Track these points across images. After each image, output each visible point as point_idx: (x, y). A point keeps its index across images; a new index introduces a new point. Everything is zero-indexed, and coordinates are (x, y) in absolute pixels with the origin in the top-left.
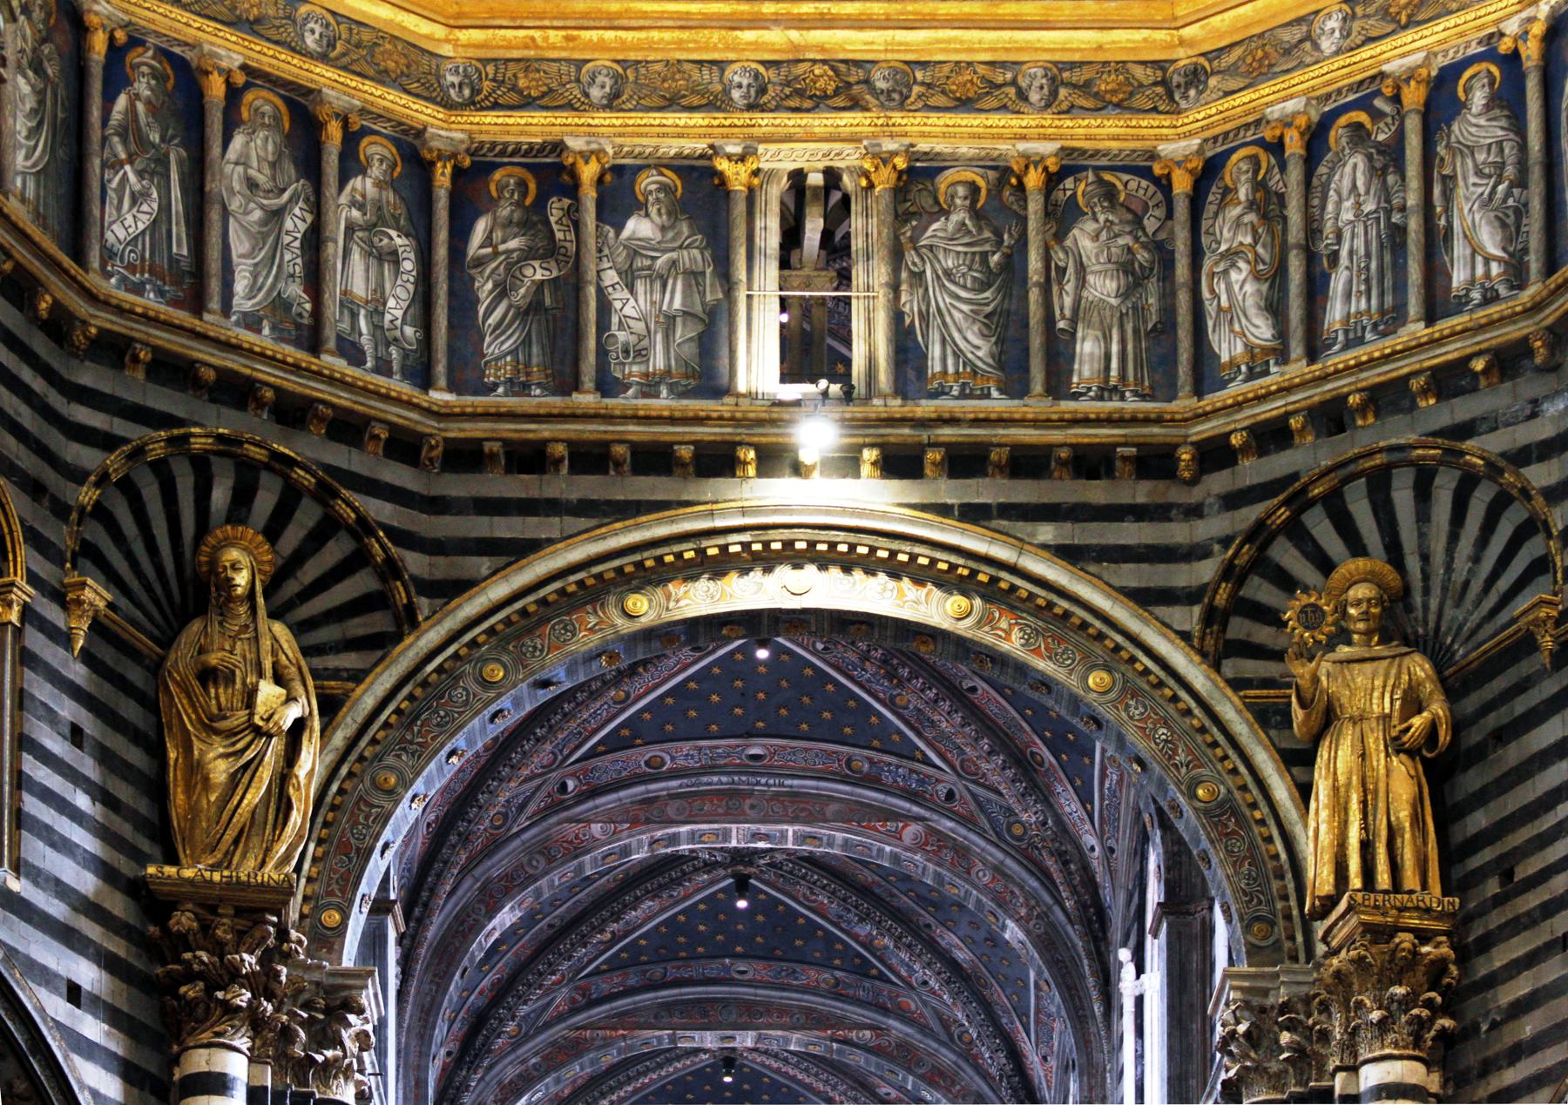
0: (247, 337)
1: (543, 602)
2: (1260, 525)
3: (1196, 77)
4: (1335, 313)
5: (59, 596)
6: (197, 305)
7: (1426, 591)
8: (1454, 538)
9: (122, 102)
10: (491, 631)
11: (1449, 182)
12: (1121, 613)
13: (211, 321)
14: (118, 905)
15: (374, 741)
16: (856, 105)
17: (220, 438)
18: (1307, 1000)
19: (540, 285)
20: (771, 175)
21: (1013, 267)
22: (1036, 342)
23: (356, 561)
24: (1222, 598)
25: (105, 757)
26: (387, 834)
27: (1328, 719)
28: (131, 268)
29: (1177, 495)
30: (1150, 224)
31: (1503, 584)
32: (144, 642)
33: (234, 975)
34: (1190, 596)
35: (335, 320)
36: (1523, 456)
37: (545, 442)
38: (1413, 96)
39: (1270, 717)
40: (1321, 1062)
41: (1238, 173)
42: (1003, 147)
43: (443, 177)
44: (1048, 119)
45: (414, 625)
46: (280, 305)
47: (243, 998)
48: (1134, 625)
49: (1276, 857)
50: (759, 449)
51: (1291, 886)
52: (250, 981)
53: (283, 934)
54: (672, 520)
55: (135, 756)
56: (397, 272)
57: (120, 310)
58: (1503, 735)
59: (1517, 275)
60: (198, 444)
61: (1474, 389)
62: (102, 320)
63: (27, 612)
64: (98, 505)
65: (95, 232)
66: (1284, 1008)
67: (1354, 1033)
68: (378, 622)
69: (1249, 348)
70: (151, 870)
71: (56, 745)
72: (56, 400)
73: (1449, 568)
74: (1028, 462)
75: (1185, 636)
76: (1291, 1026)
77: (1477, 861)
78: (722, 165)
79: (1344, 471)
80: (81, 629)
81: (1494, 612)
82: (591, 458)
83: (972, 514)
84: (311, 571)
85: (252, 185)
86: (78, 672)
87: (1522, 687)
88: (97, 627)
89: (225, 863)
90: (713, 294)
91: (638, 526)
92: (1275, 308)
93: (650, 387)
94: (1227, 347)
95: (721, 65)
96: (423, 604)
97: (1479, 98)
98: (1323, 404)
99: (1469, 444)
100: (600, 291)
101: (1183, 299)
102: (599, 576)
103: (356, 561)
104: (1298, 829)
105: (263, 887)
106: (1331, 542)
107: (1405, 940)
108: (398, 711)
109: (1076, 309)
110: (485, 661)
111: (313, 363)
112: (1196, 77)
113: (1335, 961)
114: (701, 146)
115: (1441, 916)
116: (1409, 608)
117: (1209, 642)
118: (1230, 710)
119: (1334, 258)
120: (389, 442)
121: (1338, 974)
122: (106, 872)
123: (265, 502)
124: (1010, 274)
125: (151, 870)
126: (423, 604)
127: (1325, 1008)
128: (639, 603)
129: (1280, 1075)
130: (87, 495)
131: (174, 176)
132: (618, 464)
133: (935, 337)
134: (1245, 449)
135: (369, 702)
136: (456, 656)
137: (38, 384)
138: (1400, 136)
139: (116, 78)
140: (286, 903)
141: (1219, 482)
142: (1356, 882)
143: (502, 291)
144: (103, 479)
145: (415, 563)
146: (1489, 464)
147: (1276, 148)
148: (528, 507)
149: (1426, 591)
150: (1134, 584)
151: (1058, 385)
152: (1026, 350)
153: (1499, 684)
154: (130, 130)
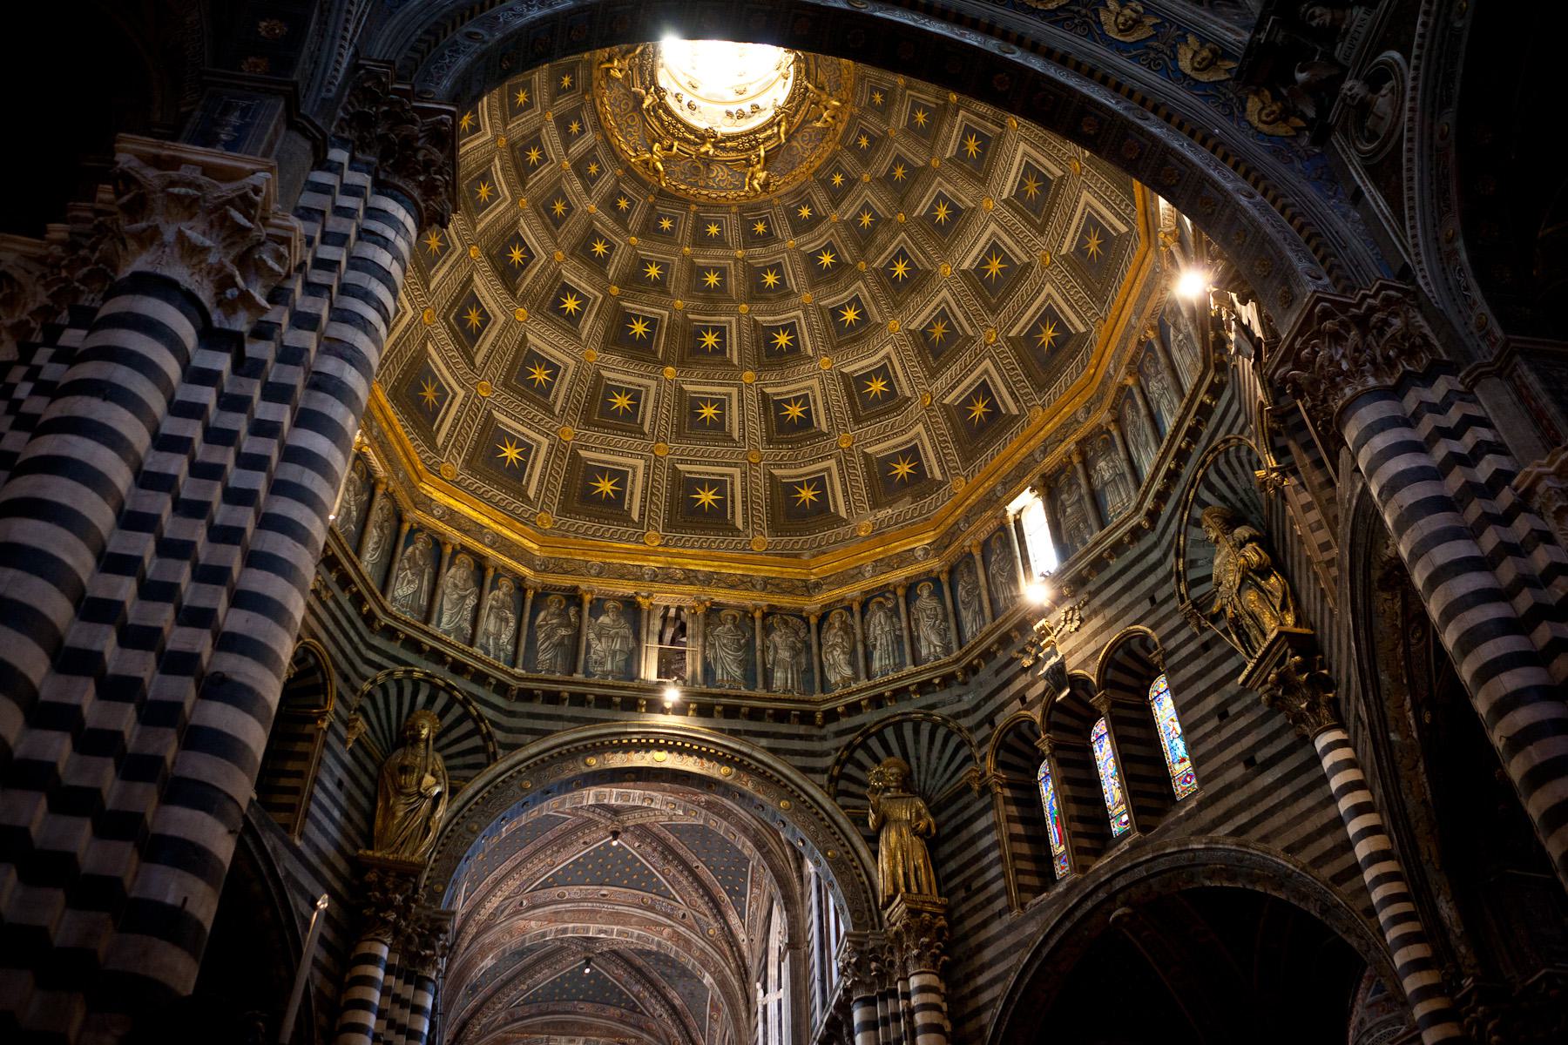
0: (444, 637)
1: (551, 757)
2: (851, 743)
3: (817, 585)
4: (876, 665)
6: (427, 621)
7: (919, 773)
8: (930, 749)
9: (410, 549)
10: (528, 767)
11: (917, 621)
12: (795, 776)
14: (342, 865)
15: (470, 810)
16: (691, 584)
17: (426, 674)
18: (882, 948)
22: (759, 669)
23: (476, 731)
24: (836, 772)
25: (350, 797)
27: (883, 821)
28: (402, 605)
29: (815, 731)
30: (802, 634)
31: (953, 767)
32: (377, 753)
33: (389, 905)
34: (823, 771)
35: (480, 639)
36: (957, 716)
37: (559, 692)
38: (900, 592)
39: (859, 821)
40: (890, 976)
43: (530, 594)
44: (763, 594)
47: (392, 917)
48: (800, 782)
49: (863, 883)
50: (647, 700)
51: (871, 896)
52: (397, 909)
53: (416, 891)
54: (610, 727)
55: (363, 801)
56: (507, 625)
57: (396, 618)
58: (957, 830)
59: (947, 650)
60: (416, 675)
62: (386, 620)
63: (331, 725)
64: (369, 692)
65: (391, 588)
66: (872, 951)
68: (481, 758)
69: (842, 677)
70: (361, 852)
71: (330, 786)
73: (929, 763)
74: (755, 714)
75: (822, 787)
76: (876, 959)
79: (884, 723)
81: (949, 779)
82: (579, 700)
83: (734, 733)
84: (454, 734)
85: (456, 586)
86: (347, 758)
88: (358, 741)
89: (397, 851)
90: (632, 643)
91: (595, 728)
92: (852, 663)
93: (605, 675)
94: (833, 678)
96: (500, 752)
97: (925, 593)
98: (875, 696)
99: (934, 712)
101: (816, 659)
102: (576, 748)
103: (476, 731)
104: (873, 871)
105: (412, 864)
106: (880, 752)
107: (926, 916)
108: (483, 798)
109: (774, 661)
110: (523, 779)
111: (470, 650)
112: (817, 585)
113: (895, 928)
114: (632, 592)
115: (941, 906)
116: (912, 780)
117: (831, 790)
119: (874, 646)
120: (496, 686)
121: (897, 933)
122: (339, 849)
123: (442, 699)
124: (749, 646)
125: (361, 852)
126: (500, 752)
127: (891, 951)
128: (593, 761)
129: (872, 984)
130: (366, 687)
131: (426, 577)
132: (589, 703)
133: (719, 666)
134: (843, 714)
135: (470, 792)
136: (511, 776)
137: (356, 639)
138: (897, 605)
139: (410, 540)
140: (421, 872)
141: (833, 727)
143: (548, 637)
144: (374, 682)
145: (499, 735)
146: (943, 719)
147: (849, 609)
148: (549, 717)
149: (919, 773)
150: (799, 764)
151: (768, 684)
152: (755, 674)
153: (954, 808)
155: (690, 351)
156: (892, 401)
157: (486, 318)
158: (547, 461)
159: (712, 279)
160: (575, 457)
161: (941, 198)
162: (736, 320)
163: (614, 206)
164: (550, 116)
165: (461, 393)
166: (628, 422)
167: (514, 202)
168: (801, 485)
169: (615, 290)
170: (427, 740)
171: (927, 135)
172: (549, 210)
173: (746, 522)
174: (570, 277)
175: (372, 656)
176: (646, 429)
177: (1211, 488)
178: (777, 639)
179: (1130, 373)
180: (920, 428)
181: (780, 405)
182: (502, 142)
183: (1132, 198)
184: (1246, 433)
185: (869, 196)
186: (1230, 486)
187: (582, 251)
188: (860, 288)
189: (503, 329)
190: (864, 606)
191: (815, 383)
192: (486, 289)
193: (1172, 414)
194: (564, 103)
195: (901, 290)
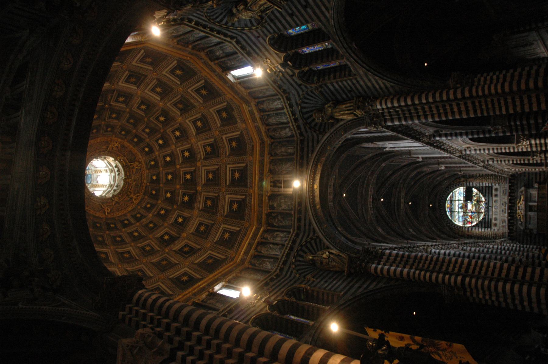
0: (282, 253)
1: (317, 219)
4: (285, 121)
5: (308, 281)
6: (278, 259)
8: (310, 103)
9: (257, 265)
11: (271, 109)
12: (320, 145)
13: (279, 257)
14: (349, 279)
19: (281, 218)
20: (271, 189)
21: (280, 160)
24: (318, 132)
25: (330, 278)
26: (345, 242)
27: (332, 117)
30: (277, 144)
35: (282, 242)
36: (299, 96)
38: (262, 114)
39: (332, 125)
41: (271, 134)
42: (268, 162)
45: (318, 236)
46: (280, 249)
48: (321, 143)
49: (351, 123)
53: (356, 258)
57: (277, 268)
58: (333, 94)
59: (279, 99)
60: (294, 261)
61: (292, 102)
62: (278, 271)
66: (370, 120)
67: (373, 110)
68: (318, 240)
69: (290, 131)
72: (286, 278)
75: (323, 137)
76: (373, 119)
77: (350, 96)
78: (269, 195)
80: (312, 279)
84: (311, 249)
85: (267, 251)
86: (318, 280)
87: (327, 92)
88: (313, 277)
92: (285, 128)
94: (290, 134)
95: (259, 195)
97: (262, 106)
100: (282, 210)
103: (310, 242)
106: (312, 118)
118: (332, 130)
119: (279, 121)
123: (302, 253)
125: (345, 274)
126: (316, 235)
127: (370, 114)
128: (318, 207)
130: (298, 276)
141: (304, 133)
142: (352, 111)
143: (281, 222)
145: (311, 235)
147: (268, 130)
148: (305, 220)
154: (260, 264)
155: (193, 182)
156: (203, 119)
157: (186, 245)
158: (228, 225)
159: (170, 177)
160: (226, 216)
161: (138, 108)
162: (181, 169)
163: (150, 208)
164: (123, 230)
165: (209, 252)
166: (215, 201)
167: (151, 239)
168: (231, 146)
169: (175, 207)
170: (313, 257)
171: (119, 114)
172: (152, 228)
173: (244, 163)
174: (172, 221)
175: (288, 275)
176: (216, 195)
177: (221, 20)
178: (279, 151)
179: (188, 47)
180: (211, 110)
181: (207, 154)
182: (132, 244)
183: (133, 49)
184: (202, 10)
185: (140, 130)
186: (220, 15)
187: (164, 218)
188: (169, 131)
189: (190, 240)
190: (267, 125)
191: (199, 143)
192: (177, 246)
193: (198, 34)
194: (119, 225)
195: (169, 119)
